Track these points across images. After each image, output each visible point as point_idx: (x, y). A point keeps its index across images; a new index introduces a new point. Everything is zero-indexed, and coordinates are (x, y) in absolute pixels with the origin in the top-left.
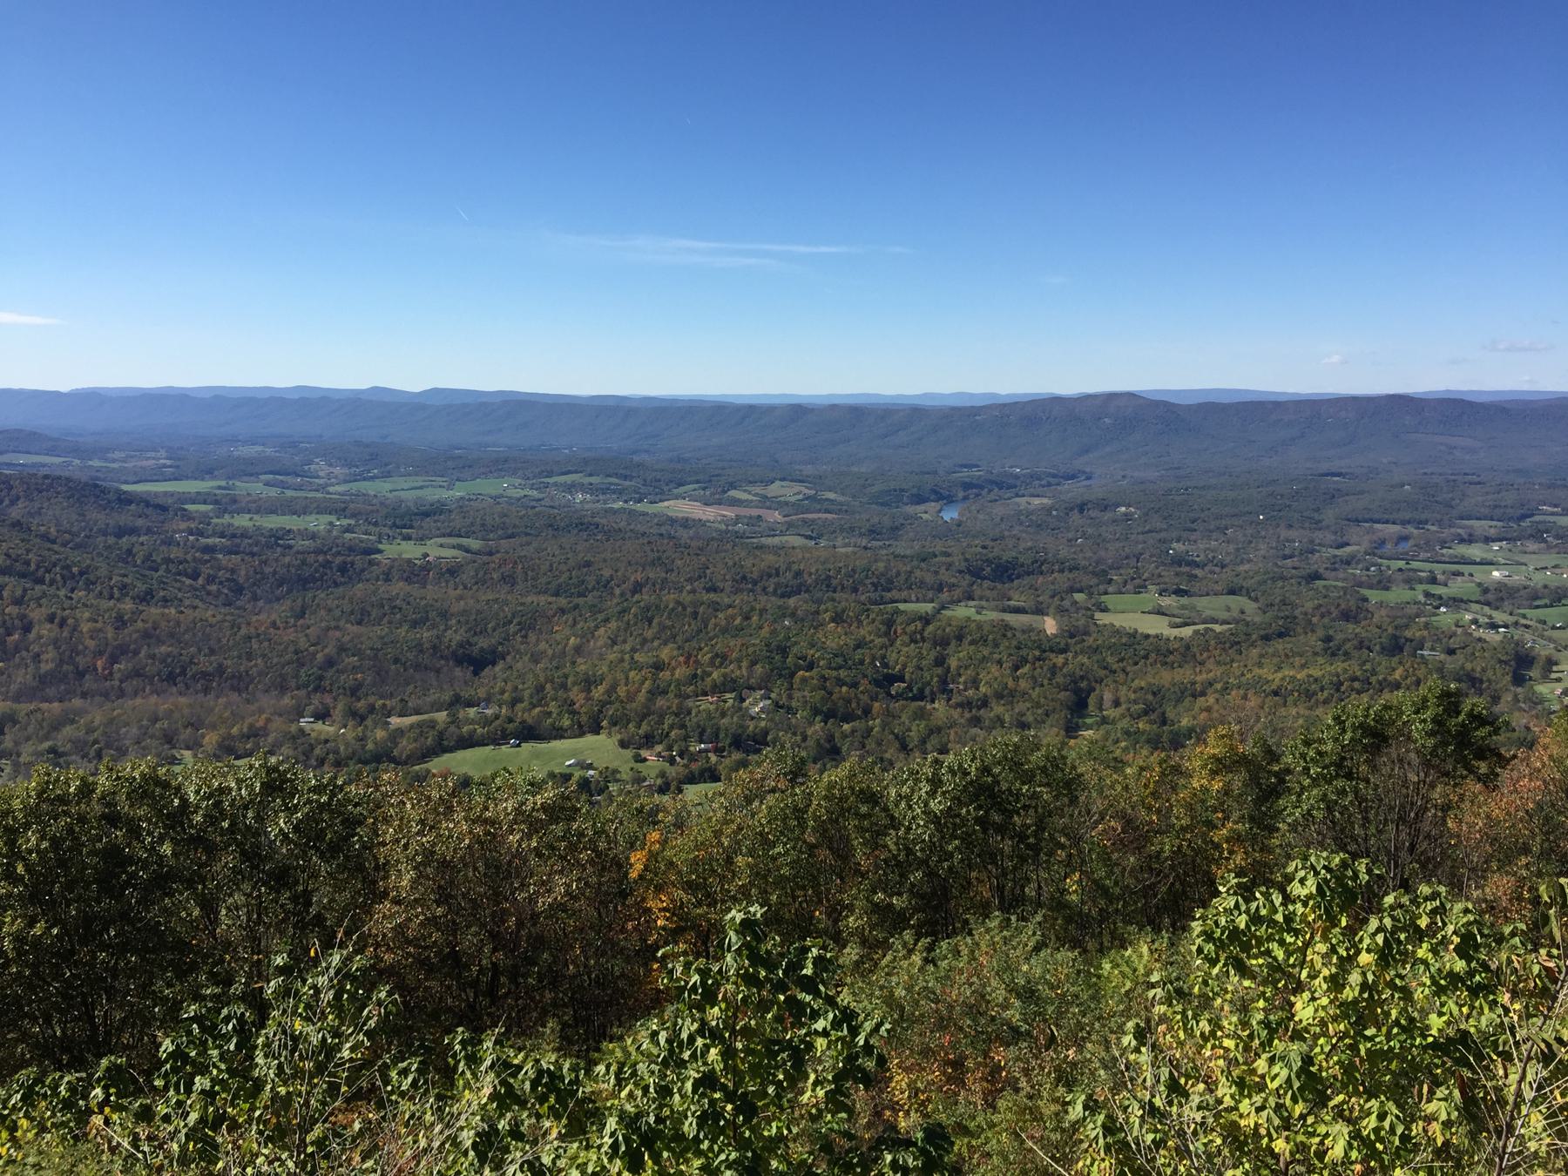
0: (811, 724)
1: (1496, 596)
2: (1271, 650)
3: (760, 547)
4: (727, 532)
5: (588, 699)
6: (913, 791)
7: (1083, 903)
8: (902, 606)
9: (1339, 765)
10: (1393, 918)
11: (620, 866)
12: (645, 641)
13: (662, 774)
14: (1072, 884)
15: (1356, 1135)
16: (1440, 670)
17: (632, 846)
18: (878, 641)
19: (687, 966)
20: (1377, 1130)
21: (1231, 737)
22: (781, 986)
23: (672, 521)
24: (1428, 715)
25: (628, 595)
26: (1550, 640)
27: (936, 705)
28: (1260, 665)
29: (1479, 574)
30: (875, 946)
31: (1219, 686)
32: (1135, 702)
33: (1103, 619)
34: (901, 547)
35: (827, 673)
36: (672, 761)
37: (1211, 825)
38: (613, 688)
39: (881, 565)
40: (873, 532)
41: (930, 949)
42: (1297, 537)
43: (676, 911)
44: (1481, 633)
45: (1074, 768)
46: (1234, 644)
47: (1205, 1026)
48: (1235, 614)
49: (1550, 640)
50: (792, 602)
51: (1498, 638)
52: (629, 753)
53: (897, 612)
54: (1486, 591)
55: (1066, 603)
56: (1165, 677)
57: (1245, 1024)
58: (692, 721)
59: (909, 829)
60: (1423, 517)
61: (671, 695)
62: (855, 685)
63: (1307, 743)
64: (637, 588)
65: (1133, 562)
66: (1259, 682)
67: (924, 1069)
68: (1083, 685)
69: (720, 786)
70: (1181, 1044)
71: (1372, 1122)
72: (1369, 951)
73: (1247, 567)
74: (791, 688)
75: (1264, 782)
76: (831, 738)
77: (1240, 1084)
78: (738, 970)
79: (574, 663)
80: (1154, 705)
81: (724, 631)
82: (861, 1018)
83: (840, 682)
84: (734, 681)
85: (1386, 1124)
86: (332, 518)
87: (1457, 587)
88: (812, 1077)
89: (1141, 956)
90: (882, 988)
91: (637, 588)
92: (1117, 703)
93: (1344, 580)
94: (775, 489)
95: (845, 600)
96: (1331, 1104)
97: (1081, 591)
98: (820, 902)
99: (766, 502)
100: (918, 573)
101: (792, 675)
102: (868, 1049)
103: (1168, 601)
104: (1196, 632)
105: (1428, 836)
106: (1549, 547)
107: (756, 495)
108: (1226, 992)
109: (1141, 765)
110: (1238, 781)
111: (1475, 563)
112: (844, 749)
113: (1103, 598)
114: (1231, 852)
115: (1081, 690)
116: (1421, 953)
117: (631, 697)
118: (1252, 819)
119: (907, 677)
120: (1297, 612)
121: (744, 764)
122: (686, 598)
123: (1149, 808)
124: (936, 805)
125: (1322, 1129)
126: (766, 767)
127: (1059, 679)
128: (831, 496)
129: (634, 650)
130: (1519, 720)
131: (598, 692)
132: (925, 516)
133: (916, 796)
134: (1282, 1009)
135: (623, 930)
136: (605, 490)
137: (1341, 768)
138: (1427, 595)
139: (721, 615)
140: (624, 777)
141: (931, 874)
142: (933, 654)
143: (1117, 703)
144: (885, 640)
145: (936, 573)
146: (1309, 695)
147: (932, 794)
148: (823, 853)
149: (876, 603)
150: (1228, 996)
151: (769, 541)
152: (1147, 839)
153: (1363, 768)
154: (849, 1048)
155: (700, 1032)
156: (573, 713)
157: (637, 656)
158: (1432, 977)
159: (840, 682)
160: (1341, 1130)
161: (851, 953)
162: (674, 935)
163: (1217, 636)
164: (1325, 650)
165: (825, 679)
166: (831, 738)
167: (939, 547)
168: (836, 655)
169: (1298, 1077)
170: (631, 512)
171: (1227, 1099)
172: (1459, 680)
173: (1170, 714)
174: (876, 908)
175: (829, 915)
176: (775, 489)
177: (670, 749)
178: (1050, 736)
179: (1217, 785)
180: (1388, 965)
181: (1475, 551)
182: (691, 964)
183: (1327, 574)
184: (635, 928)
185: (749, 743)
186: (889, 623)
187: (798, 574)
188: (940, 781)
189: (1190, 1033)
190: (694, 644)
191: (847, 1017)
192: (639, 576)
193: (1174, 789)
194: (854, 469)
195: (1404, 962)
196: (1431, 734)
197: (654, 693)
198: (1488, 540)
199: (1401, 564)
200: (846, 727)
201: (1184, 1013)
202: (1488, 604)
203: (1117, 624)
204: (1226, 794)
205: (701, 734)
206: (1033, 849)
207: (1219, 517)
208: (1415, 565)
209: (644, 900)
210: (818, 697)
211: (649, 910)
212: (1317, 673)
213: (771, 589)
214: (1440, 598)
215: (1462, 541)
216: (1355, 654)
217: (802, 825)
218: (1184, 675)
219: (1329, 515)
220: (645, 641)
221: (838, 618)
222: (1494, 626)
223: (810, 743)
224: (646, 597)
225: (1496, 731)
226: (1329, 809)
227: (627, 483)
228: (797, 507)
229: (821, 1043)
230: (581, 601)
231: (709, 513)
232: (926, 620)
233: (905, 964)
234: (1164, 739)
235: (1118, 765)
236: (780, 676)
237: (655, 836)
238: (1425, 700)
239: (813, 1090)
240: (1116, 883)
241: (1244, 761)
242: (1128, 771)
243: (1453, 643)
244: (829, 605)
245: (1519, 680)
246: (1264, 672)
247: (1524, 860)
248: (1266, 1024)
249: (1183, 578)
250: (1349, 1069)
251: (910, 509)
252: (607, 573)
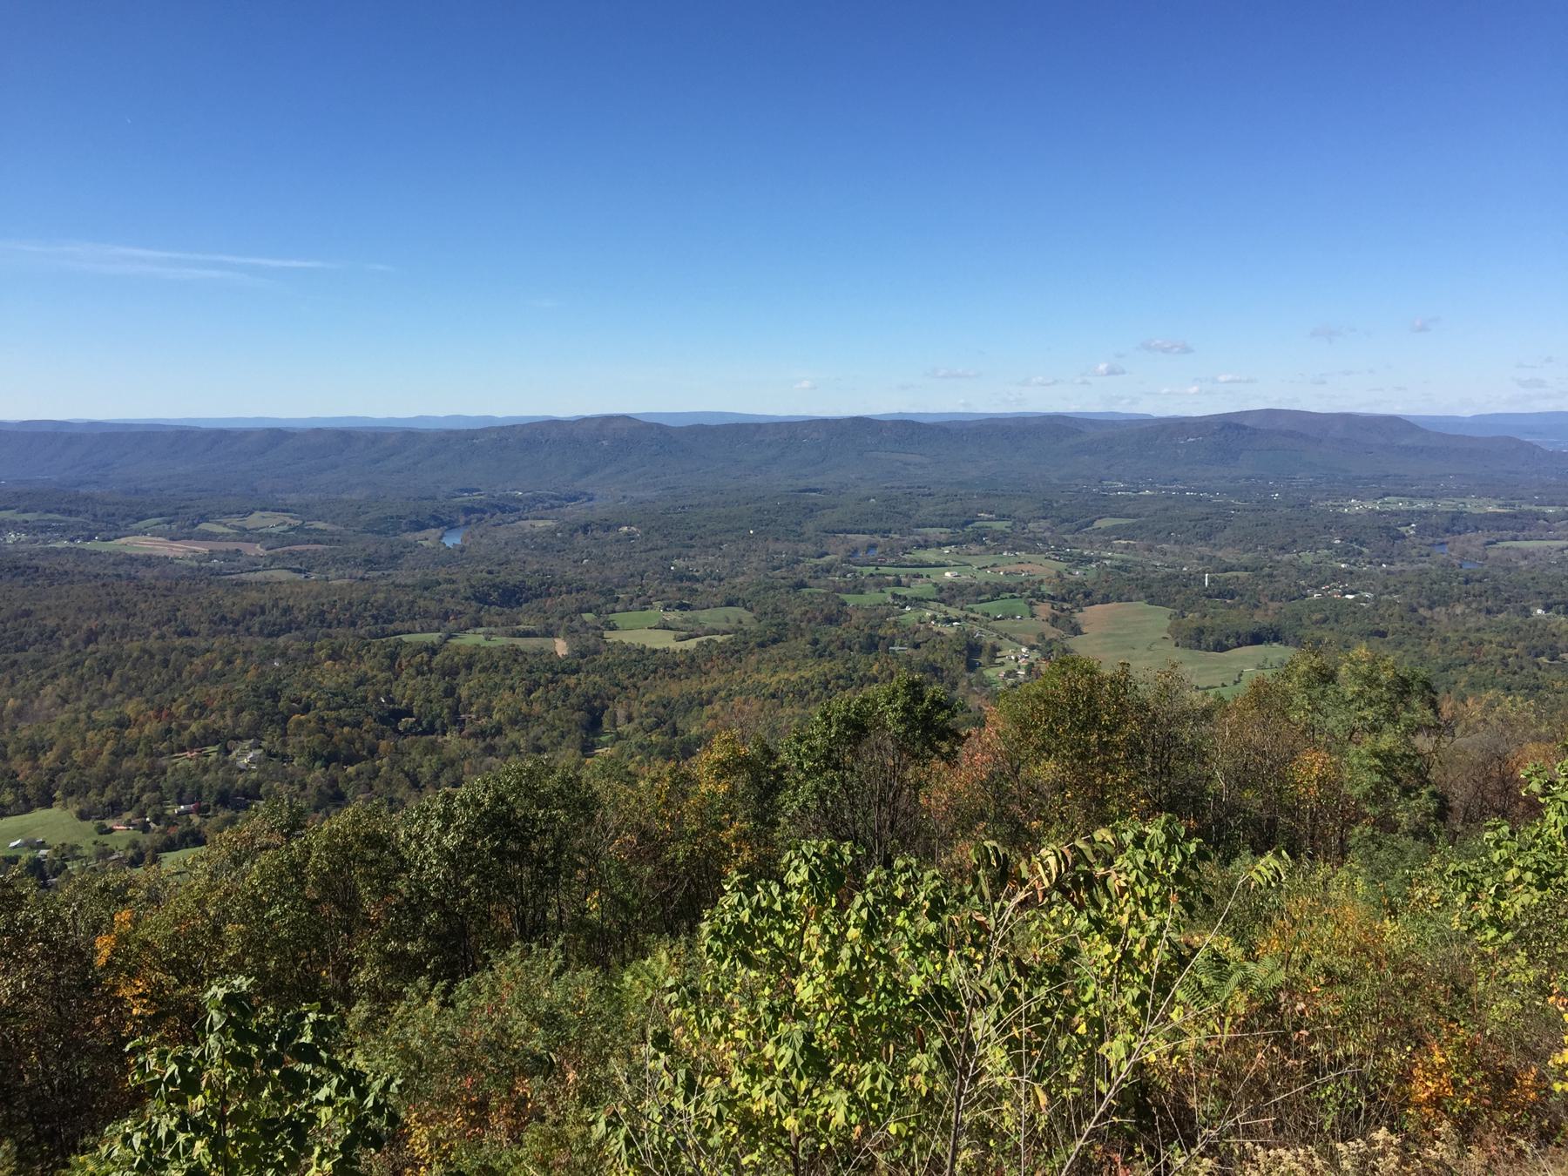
0: (310, 770)
2: (767, 656)
3: (241, 584)
4: (200, 569)
5: (34, 768)
6: (424, 830)
7: (603, 919)
8: (405, 638)
9: (828, 758)
10: (875, 893)
11: (81, 954)
12: (104, 696)
13: (134, 844)
14: (592, 903)
15: (854, 1100)
16: (909, 663)
17: (96, 929)
18: (381, 676)
19: (162, 1056)
20: (871, 1092)
21: (733, 741)
22: (275, 1061)
23: (132, 560)
24: (898, 704)
25: (81, 646)
26: (993, 629)
27: (448, 737)
28: (758, 671)
30: (384, 998)
31: (723, 694)
32: (647, 716)
33: (612, 637)
34: (402, 577)
35: (326, 714)
36: (145, 828)
37: (720, 827)
38: (67, 752)
39: (381, 596)
40: (370, 563)
41: (448, 991)
42: (784, 549)
43: (156, 996)
44: (938, 627)
45: (589, 787)
46: (734, 652)
47: (717, 1021)
48: (734, 624)
49: (993, 629)
50: (281, 641)
51: (953, 631)
52: (90, 825)
53: (401, 644)
54: (941, 590)
55: (576, 624)
56: (674, 690)
57: (753, 1013)
58: (167, 782)
59: (421, 869)
60: (887, 527)
61: (140, 755)
62: (357, 724)
63: (800, 740)
64: (92, 637)
65: (638, 580)
66: (761, 686)
67: (445, 1117)
68: (597, 703)
69: (202, 851)
70: (696, 1043)
71: (866, 1084)
72: (856, 926)
73: (741, 579)
74: (285, 734)
75: (763, 779)
76: (333, 783)
77: (752, 1071)
78: (223, 1050)
79: (14, 729)
80: (664, 717)
81: (202, 678)
82: (369, 1079)
83: (341, 723)
84: (216, 732)
85: (879, 1084)
87: (918, 588)
88: (317, 1150)
89: (660, 963)
90: (396, 1041)
91: (92, 637)
92: (630, 719)
93: (825, 587)
94: (254, 521)
95: (342, 635)
96: (833, 1074)
97: (590, 611)
98: (326, 960)
99: (244, 534)
100: (421, 602)
101: (286, 719)
102: (378, 1109)
103: (673, 616)
104: (699, 644)
105: (905, 813)
106: (988, 549)
107: (233, 527)
108: (735, 985)
109: (654, 775)
110: (742, 781)
111: (931, 566)
112: (349, 794)
113: (612, 617)
114: (739, 850)
115: (595, 708)
116: (899, 922)
117: (90, 762)
118: (756, 817)
119: (415, 711)
120: (788, 619)
121: (232, 822)
122: (153, 644)
123: (663, 818)
124: (449, 842)
125: (826, 1099)
126: (257, 822)
127: (573, 700)
128: (321, 525)
129: (91, 708)
130: (974, 702)
131: (48, 759)
132: (425, 543)
133: (426, 832)
134: (785, 992)
135: (89, 1027)
136: (44, 529)
137: (830, 760)
138: (895, 596)
139: (197, 661)
140: (86, 852)
141: (447, 914)
142: (442, 685)
143: (630, 719)
144: (388, 674)
145: (441, 601)
146: (802, 695)
147: (444, 830)
148: (327, 909)
149: (376, 636)
150: (737, 989)
151: (252, 576)
152: (661, 848)
153: (848, 758)
154: (358, 1112)
155: (181, 1127)
156: (17, 786)
157: (95, 715)
158: (909, 942)
159: (341, 723)
160: (842, 1096)
161: (361, 1010)
162: (155, 1022)
163: (719, 646)
165: (323, 720)
166: (333, 783)
167: (442, 574)
168: (335, 695)
169: (802, 1055)
170: (80, 553)
171: (741, 1087)
172: (924, 672)
173: (680, 725)
174: (390, 958)
175: (336, 973)
176: (254, 521)
177: (142, 814)
178: (566, 757)
179: (723, 788)
180: (872, 936)
181: (930, 555)
182: (166, 1053)
183: (811, 582)
184: (104, 1023)
185: (236, 799)
186: (393, 657)
187: (287, 610)
188: (453, 816)
189: (704, 1031)
190: (167, 695)
191: (355, 1080)
192: (93, 624)
193: (685, 796)
194: (345, 497)
195: (886, 932)
196: (902, 721)
197: (117, 755)
198: (940, 545)
199: (872, 569)
200: (350, 770)
201: (697, 1012)
202: (943, 601)
203: (626, 641)
204: (732, 795)
205: (180, 795)
206: (551, 873)
207: (714, 533)
208: (883, 570)
209: (114, 988)
210: (316, 742)
211: (123, 999)
212: (808, 675)
213: (256, 629)
215: (920, 547)
216: (839, 653)
217: (301, 882)
218: (692, 685)
219: (810, 527)
220: (104, 696)
221: (335, 656)
222: (949, 621)
223: (311, 791)
224: (102, 647)
225: (953, 714)
226: (822, 800)
227: (72, 519)
228: (282, 539)
229: (325, 1113)
230: (19, 656)
231: (177, 550)
232: (433, 650)
233: (420, 1012)
234: (676, 749)
235: (631, 779)
236: (272, 721)
237: (124, 915)
238: (895, 691)
239: (319, 1165)
240: (635, 895)
241: (746, 763)
242: (642, 784)
243: (918, 638)
244: (325, 642)
245: (971, 667)
246: (764, 677)
247: (982, 825)
248: (771, 1009)
249: (685, 594)
250: (844, 1039)
251: (409, 537)
252: (51, 623)
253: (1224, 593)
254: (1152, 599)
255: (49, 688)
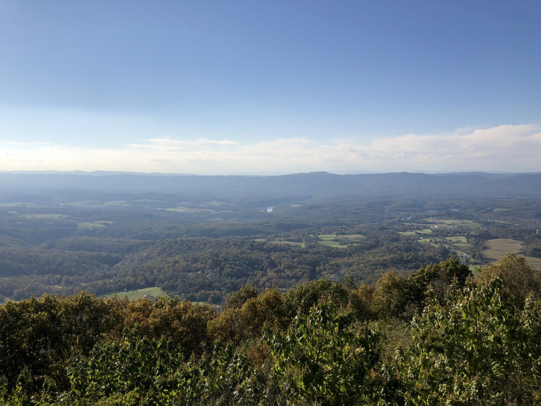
1: (437, 233)
44: (432, 245)
53: (255, 242)
86: (61, 215)
138: (417, 233)
164: (387, 251)
181: (430, 220)
199: (408, 224)
212: (386, 258)
214: (420, 234)
218: (345, 260)
222: (436, 242)
232: (264, 244)
254: (515, 238)
255: (155, 251)
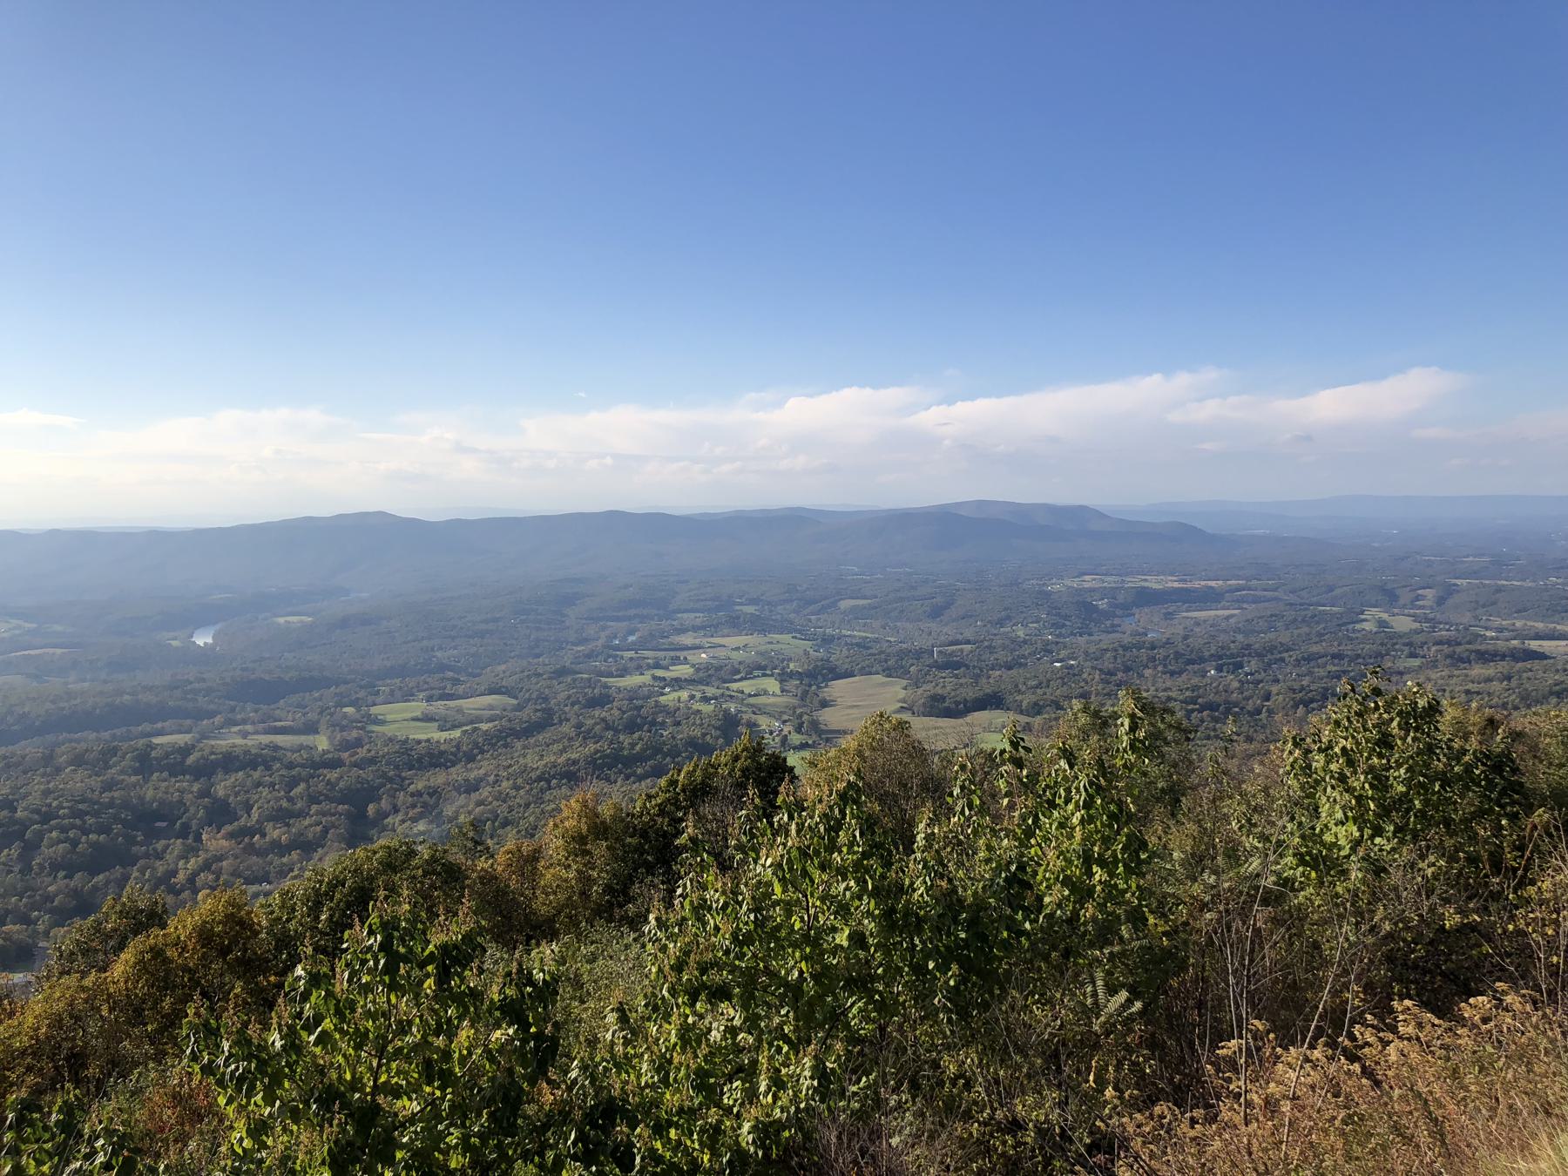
1: (707, 674)
8: (156, 740)
29: (692, 657)
44: (696, 706)
53: (152, 747)
138: (655, 678)
164: (578, 735)
181: (687, 639)
199: (631, 654)
212: (574, 756)
214: (664, 679)
218: (457, 773)
222: (706, 699)
232: (186, 751)
253: (951, 665)
